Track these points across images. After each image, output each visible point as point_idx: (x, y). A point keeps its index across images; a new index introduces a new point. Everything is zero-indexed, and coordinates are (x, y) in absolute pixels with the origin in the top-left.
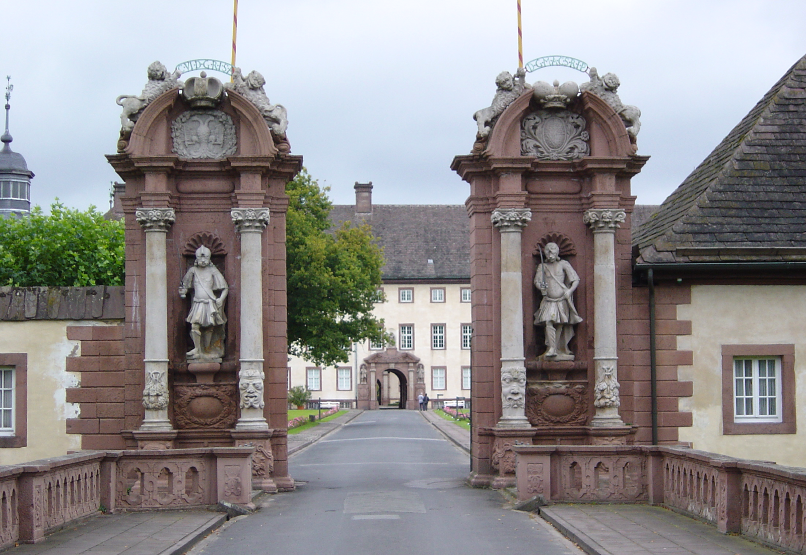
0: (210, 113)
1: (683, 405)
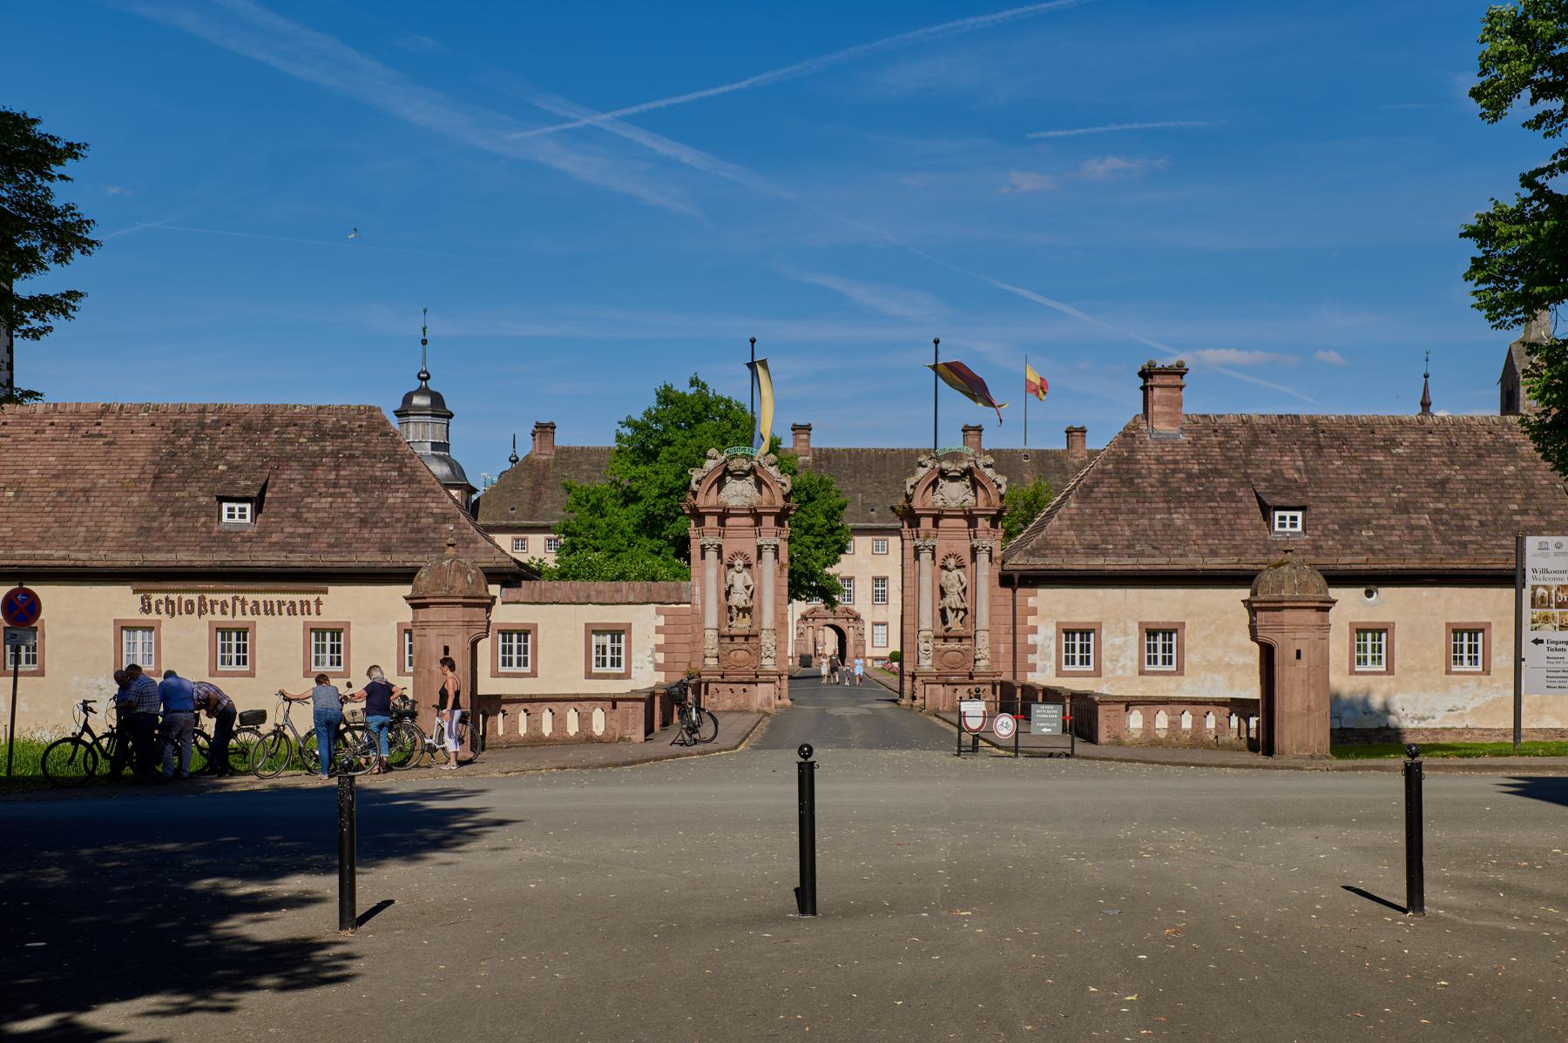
1: (1031, 659)
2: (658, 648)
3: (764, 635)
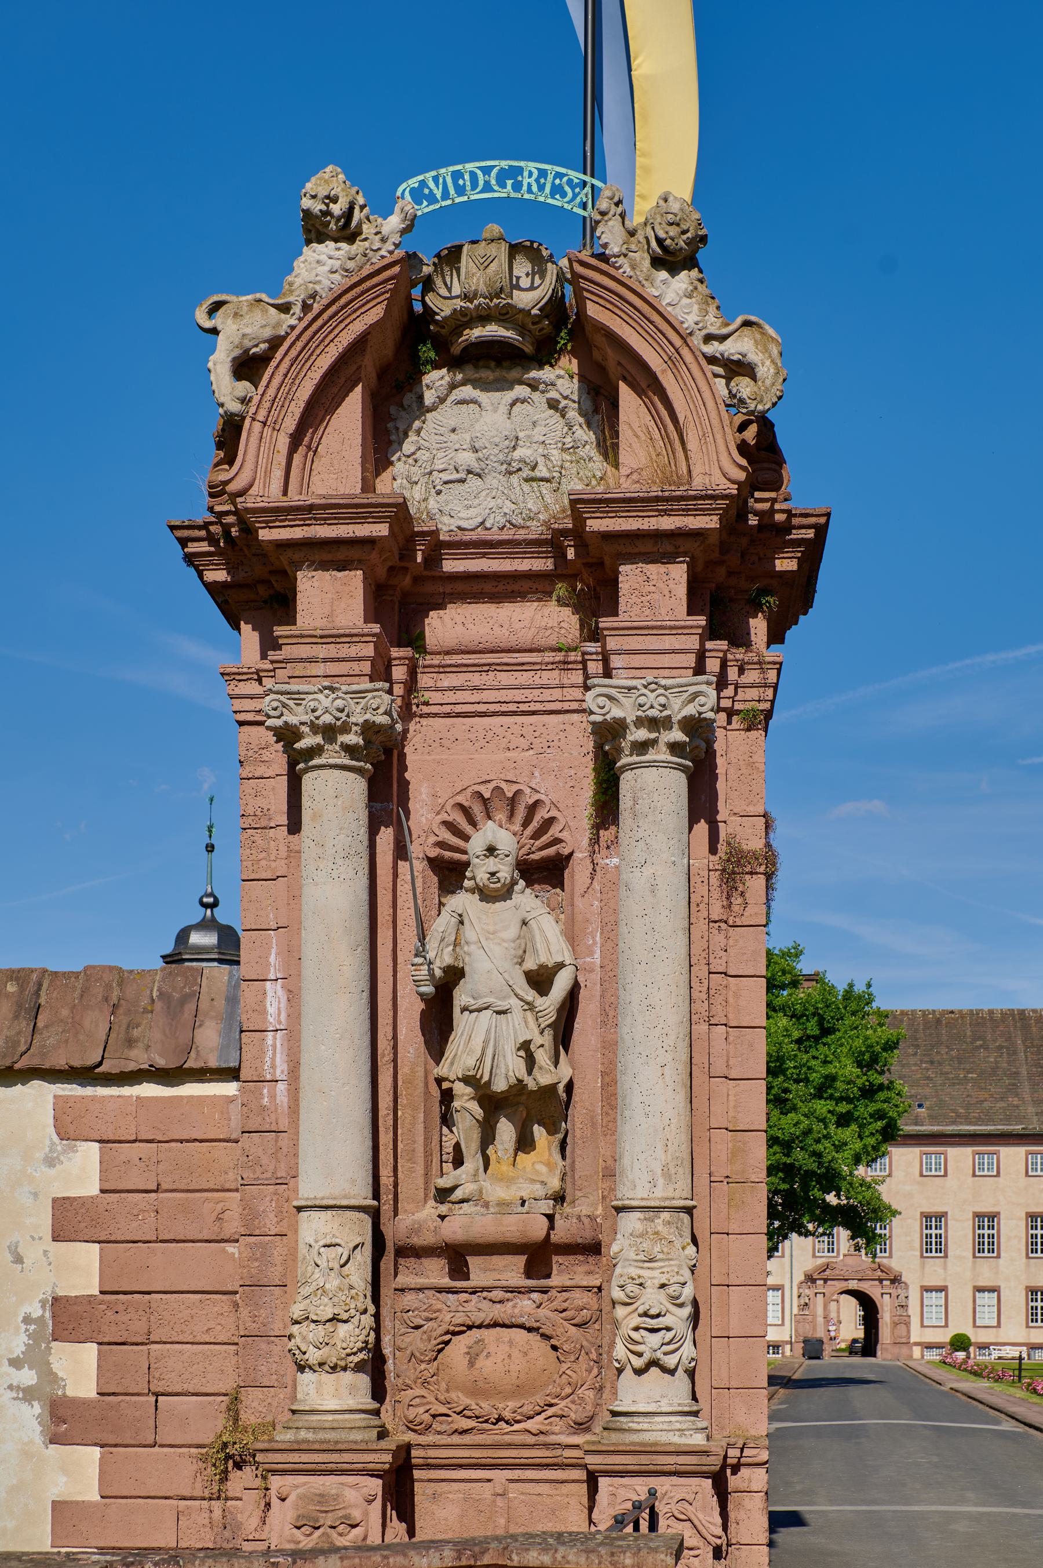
0: (515, 373)
2: (67, 1319)
3: (625, 1241)
